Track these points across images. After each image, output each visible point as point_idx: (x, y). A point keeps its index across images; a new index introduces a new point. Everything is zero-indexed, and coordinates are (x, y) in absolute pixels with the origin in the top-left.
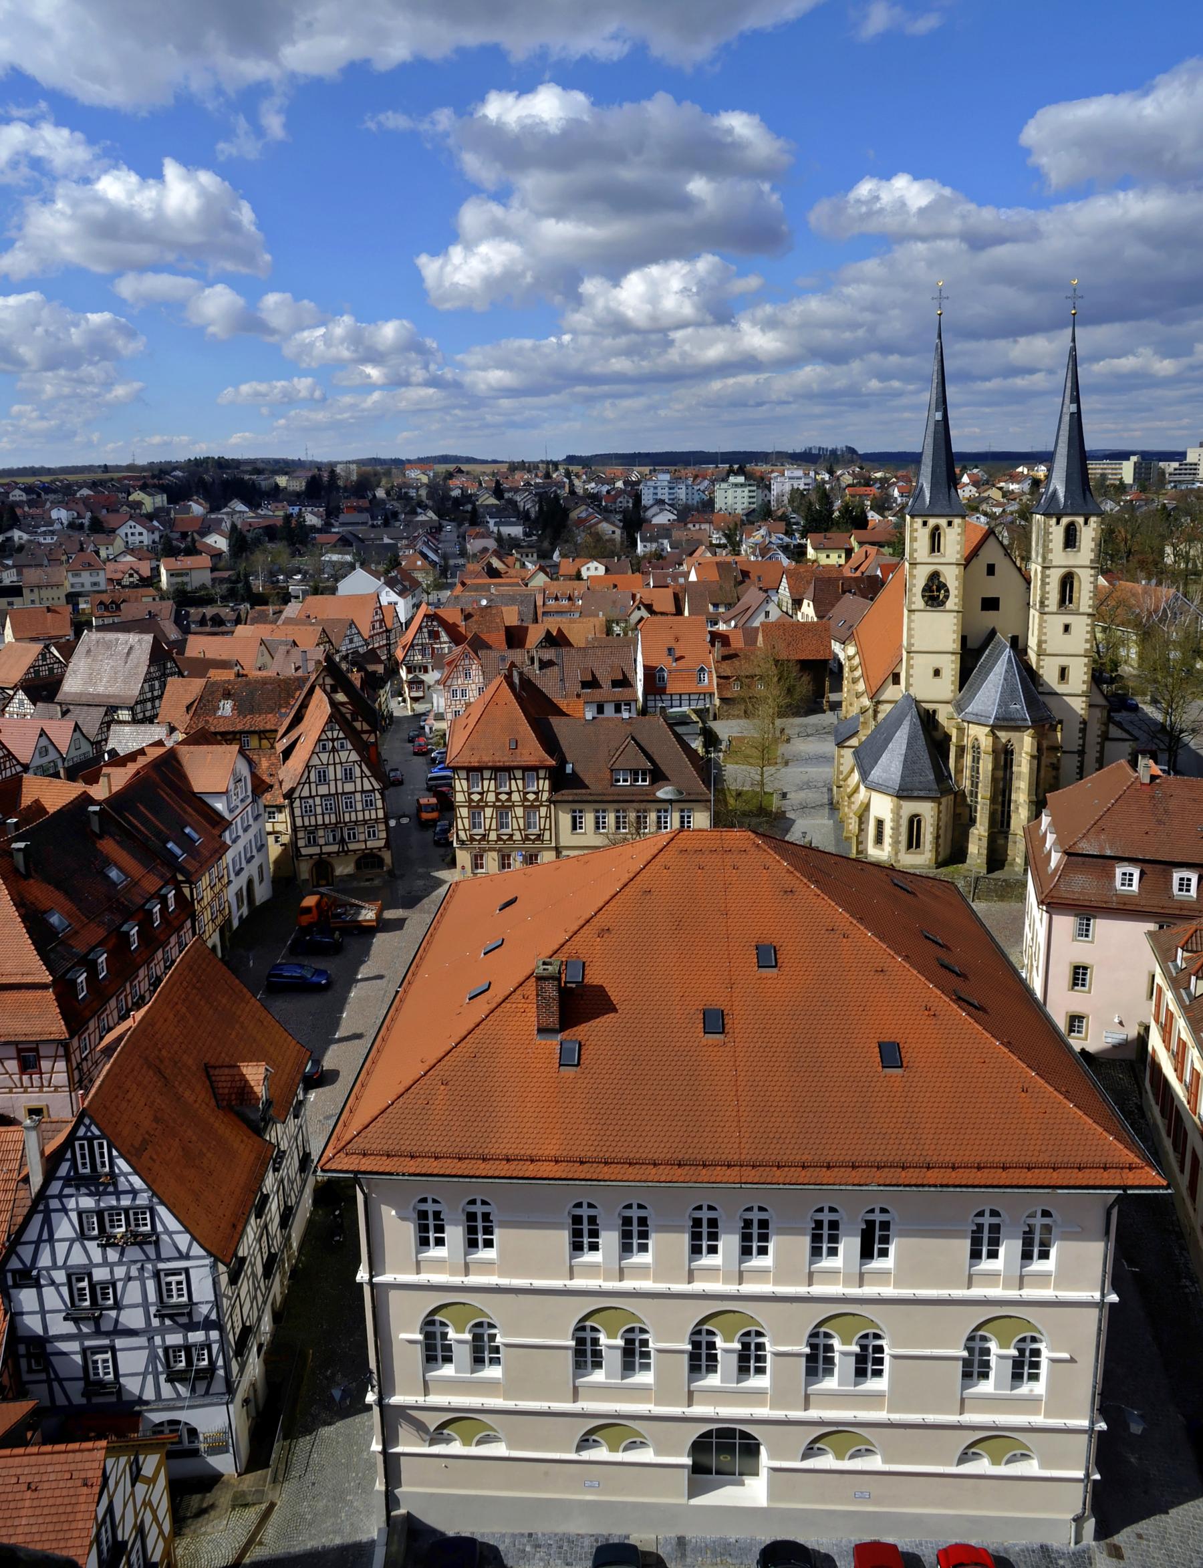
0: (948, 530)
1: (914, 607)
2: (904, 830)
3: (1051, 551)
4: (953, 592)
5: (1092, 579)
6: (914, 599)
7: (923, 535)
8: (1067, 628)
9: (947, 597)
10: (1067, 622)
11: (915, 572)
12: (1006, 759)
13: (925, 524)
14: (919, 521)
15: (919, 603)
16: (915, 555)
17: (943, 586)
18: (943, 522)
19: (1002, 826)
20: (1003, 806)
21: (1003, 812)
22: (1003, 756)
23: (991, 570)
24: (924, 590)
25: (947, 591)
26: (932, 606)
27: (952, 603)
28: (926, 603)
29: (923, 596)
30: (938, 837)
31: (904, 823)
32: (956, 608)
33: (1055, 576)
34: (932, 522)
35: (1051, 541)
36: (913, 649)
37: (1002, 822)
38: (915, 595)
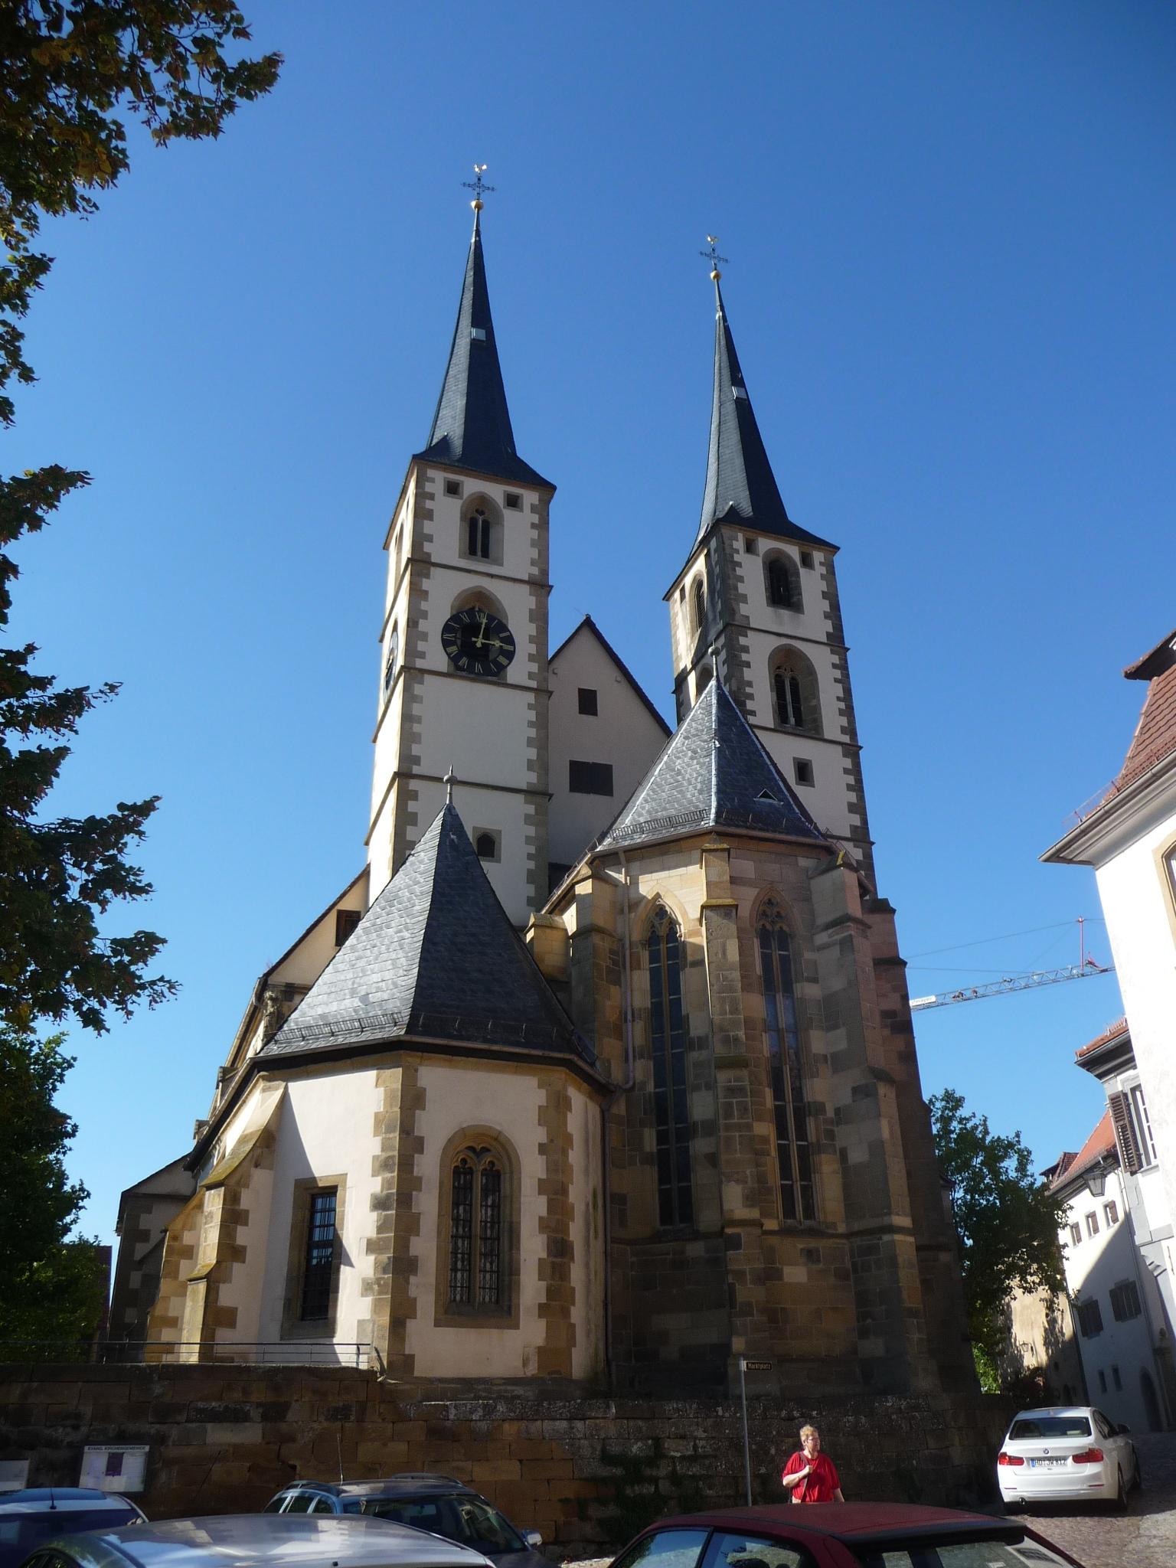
0: (508, 514)
1: (420, 663)
2: (429, 1204)
3: (744, 599)
4: (524, 647)
5: (838, 674)
6: (421, 646)
7: (449, 514)
8: (804, 771)
9: (510, 656)
10: (804, 755)
11: (426, 584)
12: (766, 960)
13: (453, 489)
14: (438, 478)
15: (437, 657)
16: (427, 547)
17: (498, 627)
18: (496, 491)
19: (789, 1211)
20: (782, 1132)
21: (783, 1152)
22: (756, 943)
23: (588, 702)
24: (447, 628)
25: (510, 640)
26: (470, 669)
27: (519, 670)
28: (454, 659)
29: (446, 644)
30: (559, 1249)
31: (430, 1166)
32: (534, 684)
33: (758, 651)
34: (472, 486)
35: (741, 579)
36: (416, 770)
37: (787, 1193)
38: (424, 637)
